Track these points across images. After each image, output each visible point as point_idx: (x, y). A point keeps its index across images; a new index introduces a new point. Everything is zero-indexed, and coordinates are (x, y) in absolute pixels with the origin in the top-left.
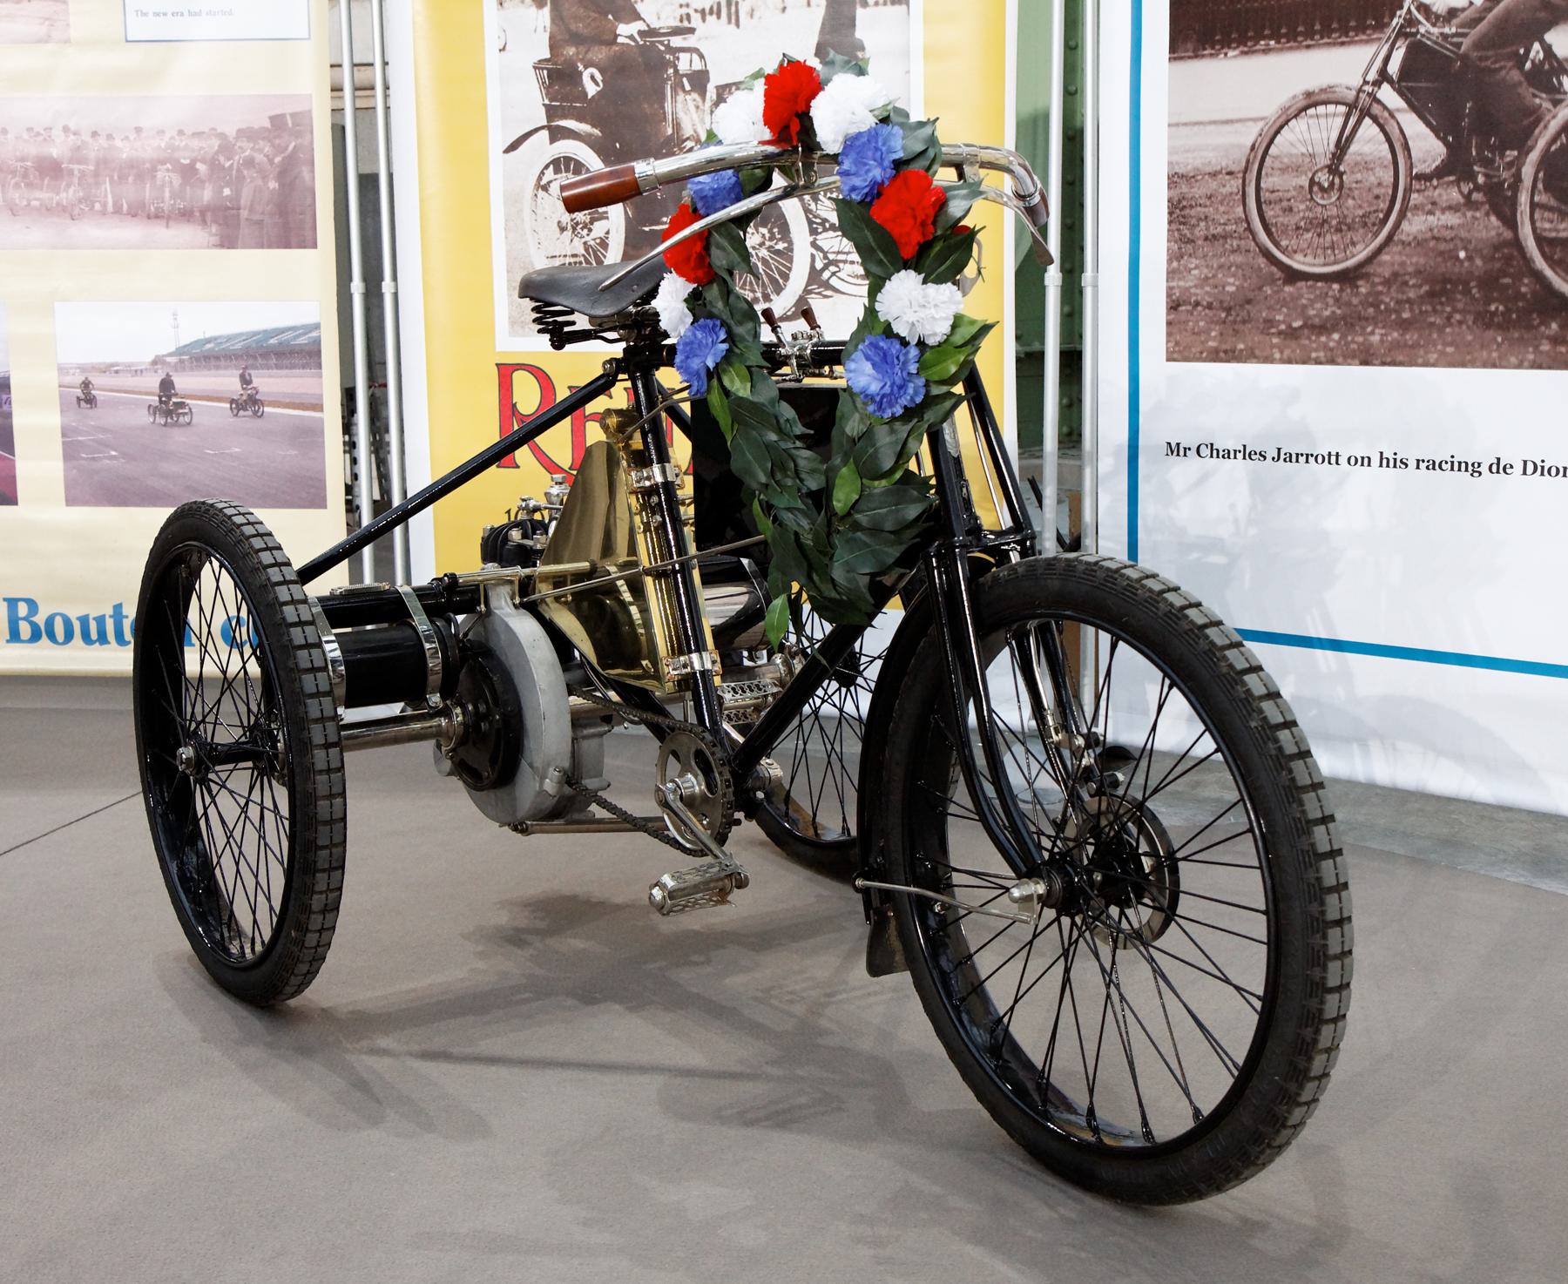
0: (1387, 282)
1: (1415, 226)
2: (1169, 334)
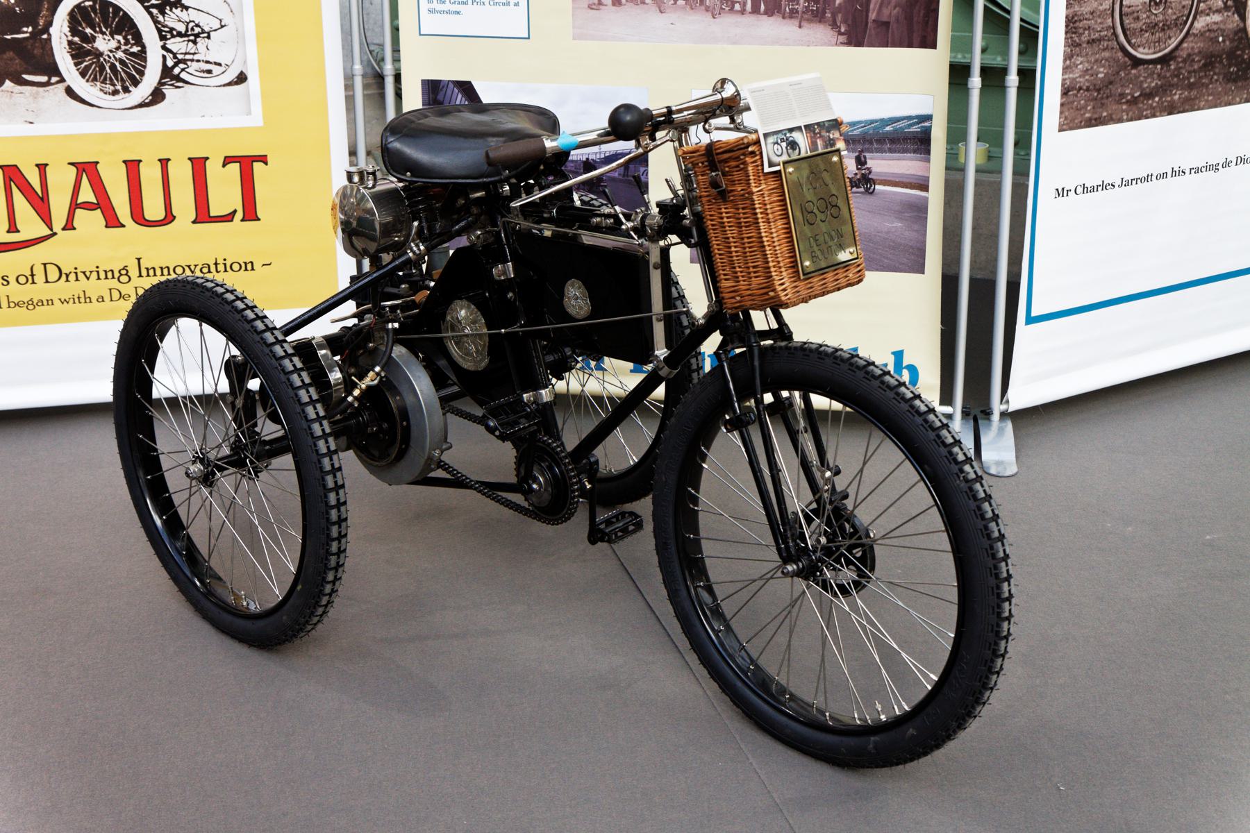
0: (1184, 61)
1: (1201, 23)
2: (1061, 113)
